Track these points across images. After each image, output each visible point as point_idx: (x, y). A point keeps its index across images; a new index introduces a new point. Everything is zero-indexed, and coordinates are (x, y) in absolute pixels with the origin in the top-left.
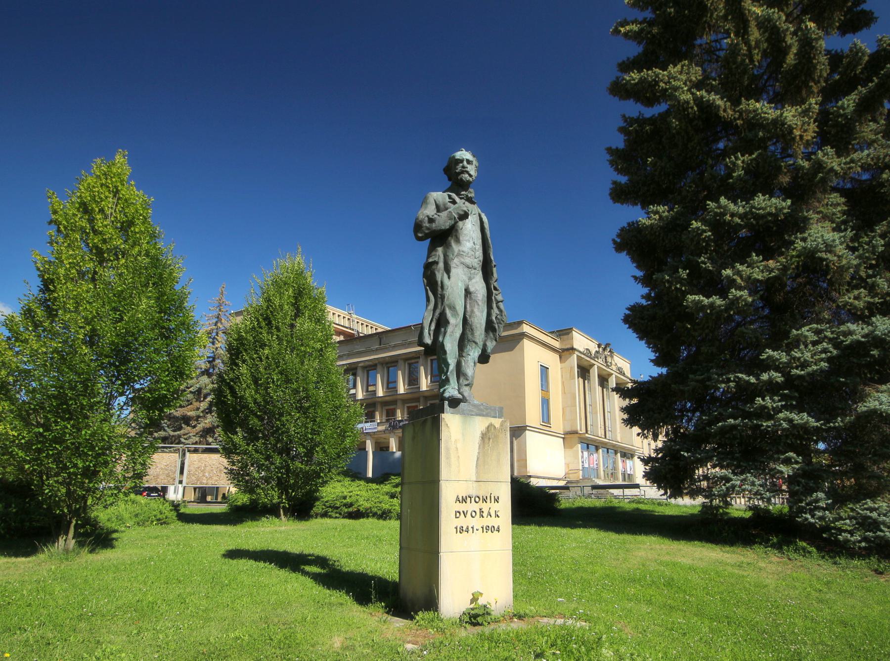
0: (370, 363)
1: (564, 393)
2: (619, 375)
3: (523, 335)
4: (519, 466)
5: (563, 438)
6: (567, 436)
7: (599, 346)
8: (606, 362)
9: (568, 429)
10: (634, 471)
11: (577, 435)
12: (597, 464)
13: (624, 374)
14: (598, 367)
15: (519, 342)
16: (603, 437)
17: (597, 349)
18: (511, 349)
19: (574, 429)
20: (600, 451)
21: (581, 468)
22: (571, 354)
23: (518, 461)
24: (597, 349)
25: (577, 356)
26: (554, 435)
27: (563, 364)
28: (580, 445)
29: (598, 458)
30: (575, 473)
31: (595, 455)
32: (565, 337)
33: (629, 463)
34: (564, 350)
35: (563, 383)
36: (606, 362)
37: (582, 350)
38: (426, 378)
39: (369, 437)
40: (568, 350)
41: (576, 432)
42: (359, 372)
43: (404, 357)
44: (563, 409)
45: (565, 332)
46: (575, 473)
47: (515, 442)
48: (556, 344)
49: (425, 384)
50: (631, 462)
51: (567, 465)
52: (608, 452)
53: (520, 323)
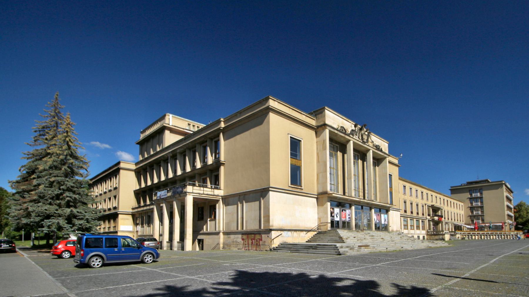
0: (182, 149)
1: (318, 161)
2: (376, 151)
3: (269, 109)
4: (264, 221)
5: (317, 198)
6: (319, 196)
7: (355, 126)
8: (362, 139)
9: (321, 191)
10: (388, 222)
11: (326, 195)
12: (349, 218)
13: (381, 151)
14: (354, 142)
15: (266, 116)
16: (362, 198)
17: (354, 128)
18: (261, 123)
19: (325, 190)
20: (353, 207)
21: (329, 221)
22: (324, 129)
23: (264, 217)
24: (354, 128)
25: (330, 131)
26: (307, 195)
27: (318, 139)
28: (329, 204)
29: (351, 213)
30: (325, 225)
31: (348, 212)
32: (320, 116)
33: (383, 217)
34: (318, 127)
35: (318, 154)
36: (362, 139)
37: (336, 127)
38: (212, 156)
39: (164, 202)
40: (321, 126)
41: (326, 193)
42: (178, 156)
43: (198, 141)
44: (317, 175)
45: (319, 112)
46: (325, 225)
47: (262, 201)
48: (313, 122)
49: (210, 160)
50: (386, 216)
51: (319, 219)
52: (362, 208)
53: (267, 99)
